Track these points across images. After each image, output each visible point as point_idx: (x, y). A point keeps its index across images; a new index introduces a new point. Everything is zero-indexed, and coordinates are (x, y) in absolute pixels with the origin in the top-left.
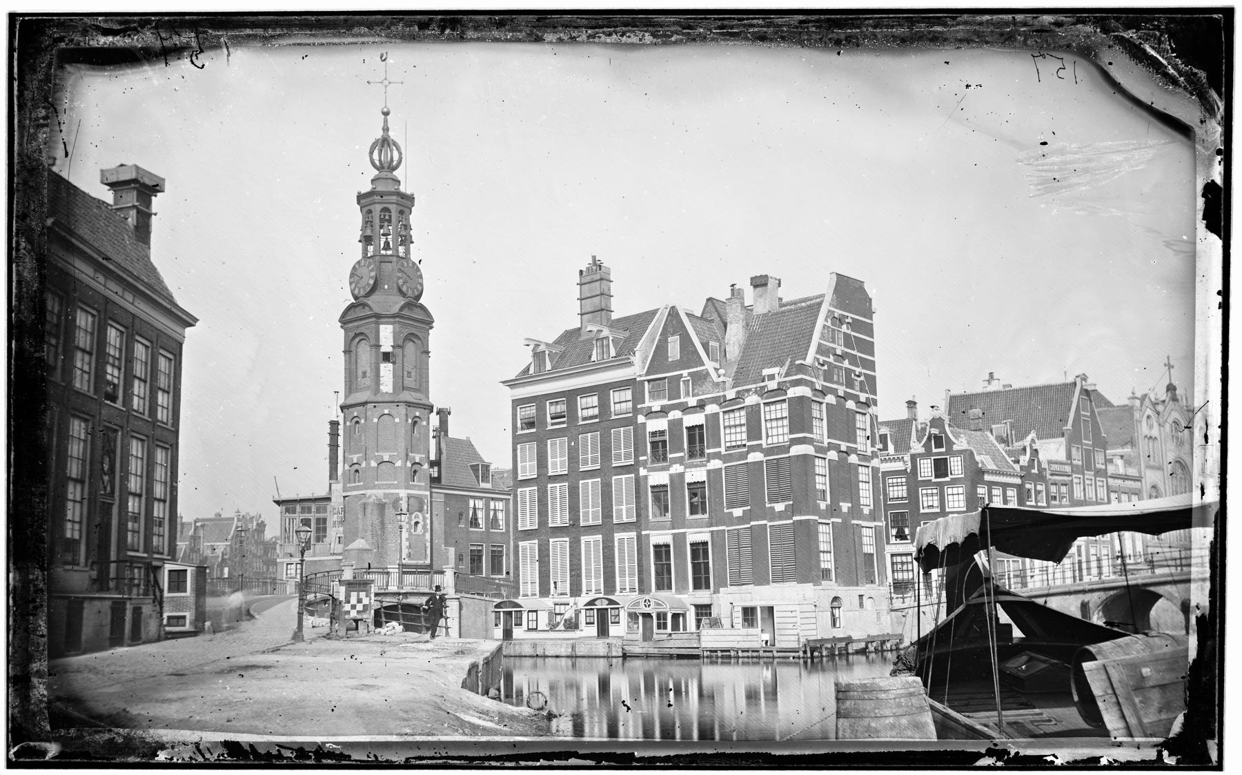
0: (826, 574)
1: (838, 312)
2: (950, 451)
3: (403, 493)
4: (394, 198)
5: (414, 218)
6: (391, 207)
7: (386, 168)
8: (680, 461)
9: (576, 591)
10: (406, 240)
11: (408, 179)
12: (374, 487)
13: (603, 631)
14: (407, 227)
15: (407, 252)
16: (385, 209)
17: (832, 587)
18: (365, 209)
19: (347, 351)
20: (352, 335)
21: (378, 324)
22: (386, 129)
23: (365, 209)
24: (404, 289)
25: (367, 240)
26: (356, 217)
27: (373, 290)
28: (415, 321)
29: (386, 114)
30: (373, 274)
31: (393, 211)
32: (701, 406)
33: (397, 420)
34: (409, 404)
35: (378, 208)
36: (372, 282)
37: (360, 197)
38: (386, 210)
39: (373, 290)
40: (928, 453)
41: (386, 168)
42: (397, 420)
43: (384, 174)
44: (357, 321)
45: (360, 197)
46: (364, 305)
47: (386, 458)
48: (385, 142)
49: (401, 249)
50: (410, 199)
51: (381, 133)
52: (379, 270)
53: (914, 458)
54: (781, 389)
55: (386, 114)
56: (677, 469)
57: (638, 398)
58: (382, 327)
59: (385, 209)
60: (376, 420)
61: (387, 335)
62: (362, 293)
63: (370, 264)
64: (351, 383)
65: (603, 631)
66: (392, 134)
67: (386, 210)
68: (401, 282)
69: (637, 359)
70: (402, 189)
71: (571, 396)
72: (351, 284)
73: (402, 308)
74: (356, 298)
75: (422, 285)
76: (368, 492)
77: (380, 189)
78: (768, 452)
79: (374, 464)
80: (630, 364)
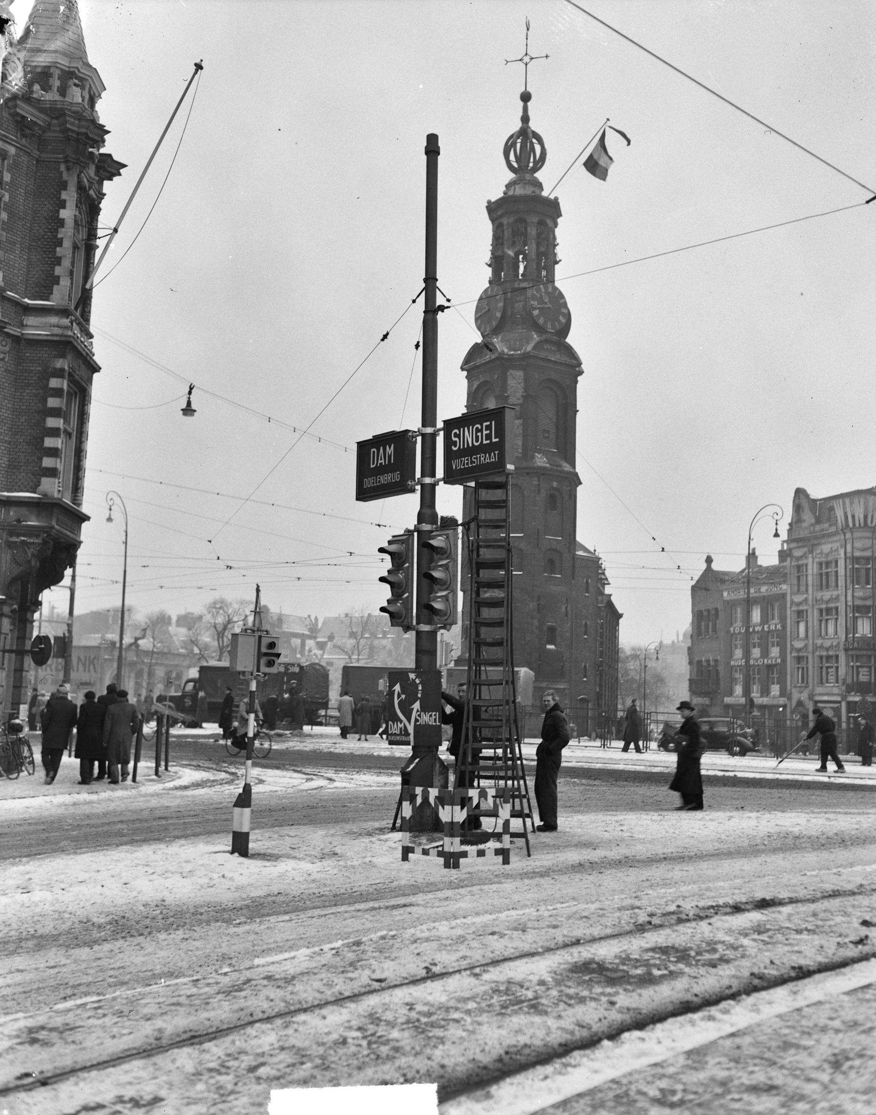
5: (564, 232)
18: (497, 223)
22: (525, 119)
24: (541, 321)
29: (526, 97)
50: (553, 209)
55: (526, 97)
59: (524, 222)
66: (533, 125)
70: (545, 194)
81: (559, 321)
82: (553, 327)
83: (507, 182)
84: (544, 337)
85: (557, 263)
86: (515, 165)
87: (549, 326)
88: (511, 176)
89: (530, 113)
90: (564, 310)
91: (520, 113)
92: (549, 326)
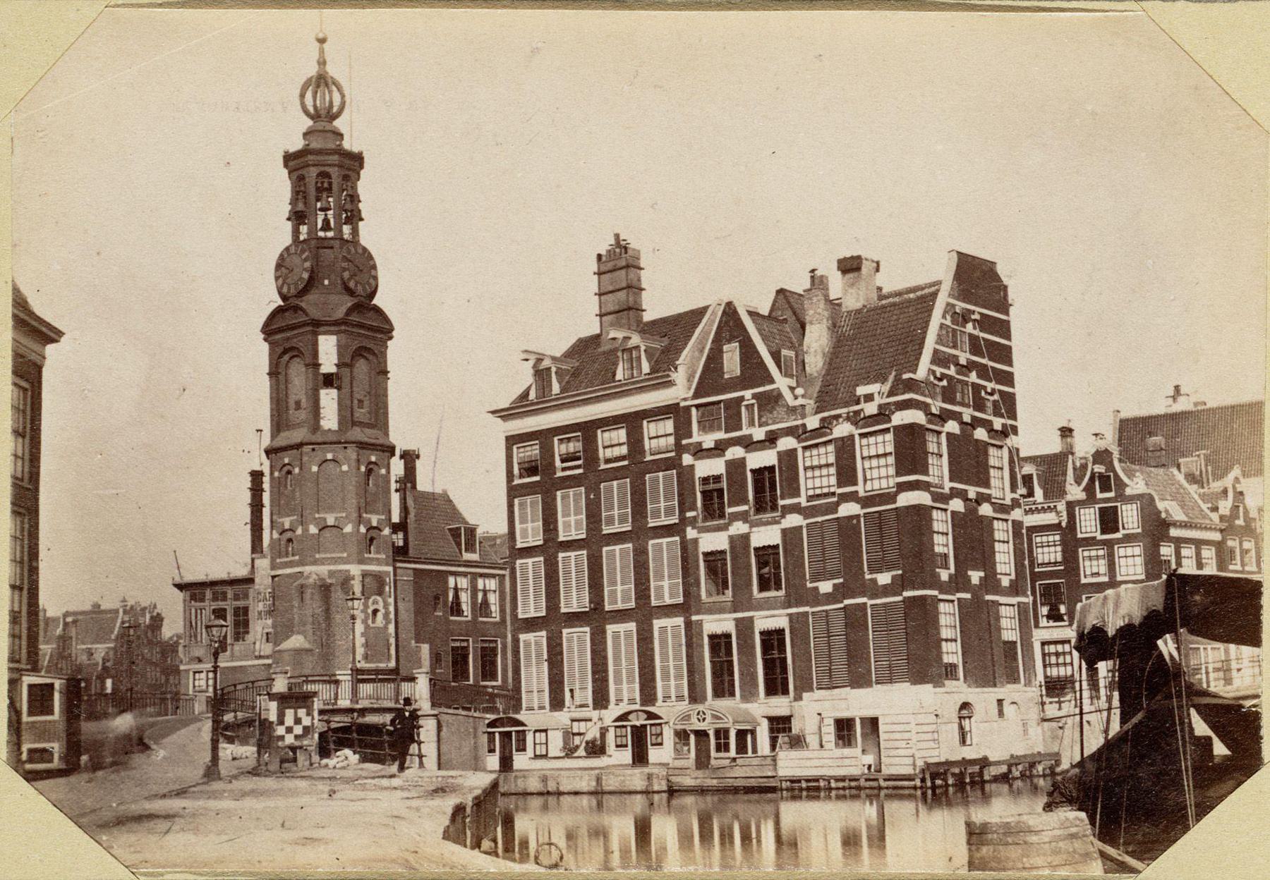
0: (950, 671)
1: (960, 306)
2: (1121, 497)
3: (355, 570)
4: (335, 158)
6: (334, 172)
7: (323, 118)
8: (744, 517)
9: (601, 700)
10: (354, 217)
11: (355, 133)
12: (315, 562)
13: (640, 758)
14: (354, 198)
15: (355, 232)
16: (324, 174)
17: (959, 690)
18: (295, 175)
19: (273, 374)
20: (279, 350)
21: (316, 334)
22: (322, 63)
23: (295, 175)
24: (352, 284)
25: (298, 217)
26: (280, 186)
28: (368, 330)
29: (322, 41)
30: (307, 264)
31: (334, 176)
32: (771, 439)
33: (345, 468)
34: (362, 445)
35: (313, 172)
36: (306, 276)
37: (288, 158)
40: (1091, 498)
41: (323, 118)
42: (345, 468)
43: (321, 125)
44: (287, 332)
45: (288, 158)
46: (297, 308)
47: (331, 521)
48: (321, 81)
49: (346, 229)
50: (355, 161)
52: (316, 258)
53: (1071, 506)
54: (883, 415)
56: (739, 528)
57: (682, 429)
58: (321, 338)
59: (324, 174)
60: (315, 469)
61: (328, 350)
62: (293, 291)
63: (303, 251)
64: (280, 421)
65: (640, 758)
66: (331, 70)
68: (346, 275)
69: (679, 376)
70: (346, 145)
71: (588, 430)
72: (277, 278)
73: (350, 311)
74: (284, 298)
75: (376, 278)
76: (307, 569)
77: (316, 144)
78: (867, 501)
79: (313, 530)
80: (670, 384)
81: (369, 284)
82: (364, 289)
84: (356, 301)
85: (362, 219)
86: (311, 110)
87: (359, 288)
88: (310, 123)
90: (373, 273)
91: (316, 56)
92: (359, 288)
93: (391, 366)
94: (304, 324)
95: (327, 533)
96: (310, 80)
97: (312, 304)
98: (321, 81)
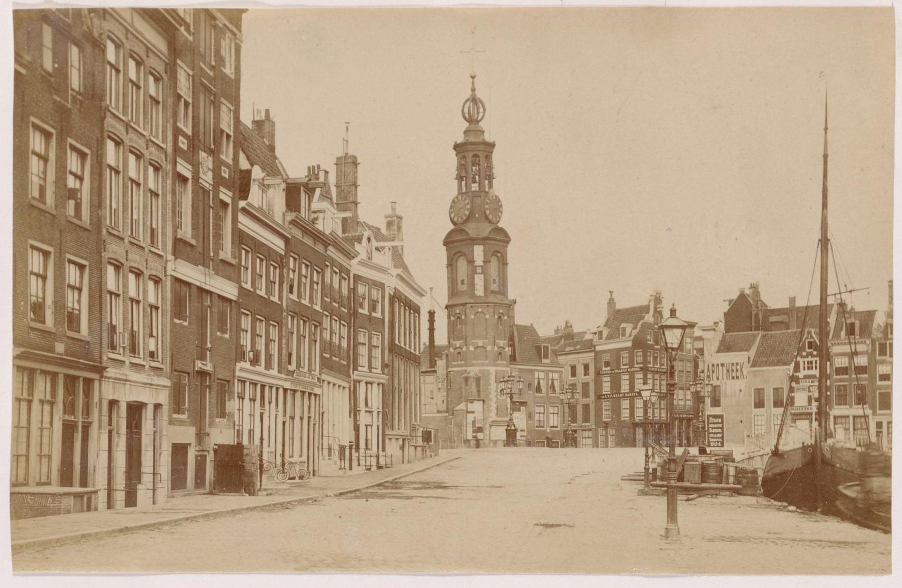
6: (481, 154)
12: (472, 365)
14: (490, 167)
16: (474, 156)
22: (473, 90)
23: (460, 155)
26: (452, 160)
27: (468, 219)
28: (498, 241)
29: (473, 77)
30: (468, 207)
35: (470, 154)
36: (467, 213)
37: (456, 147)
38: (476, 156)
39: (468, 219)
42: (487, 316)
43: (473, 127)
45: (456, 147)
46: (462, 231)
47: (480, 344)
51: (470, 93)
52: (472, 203)
55: (473, 77)
60: (473, 317)
61: (478, 252)
63: (465, 200)
66: (479, 94)
67: (476, 156)
74: (454, 223)
76: (468, 369)
77: (472, 139)
79: (472, 348)
83: (464, 129)
88: (467, 124)
89: (477, 86)
93: (510, 259)
94: (467, 240)
95: (478, 350)
96: (468, 100)
97: (472, 229)
98: (474, 100)
